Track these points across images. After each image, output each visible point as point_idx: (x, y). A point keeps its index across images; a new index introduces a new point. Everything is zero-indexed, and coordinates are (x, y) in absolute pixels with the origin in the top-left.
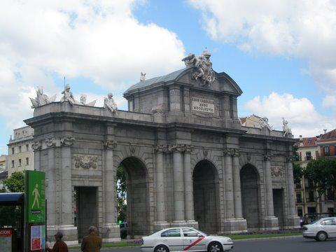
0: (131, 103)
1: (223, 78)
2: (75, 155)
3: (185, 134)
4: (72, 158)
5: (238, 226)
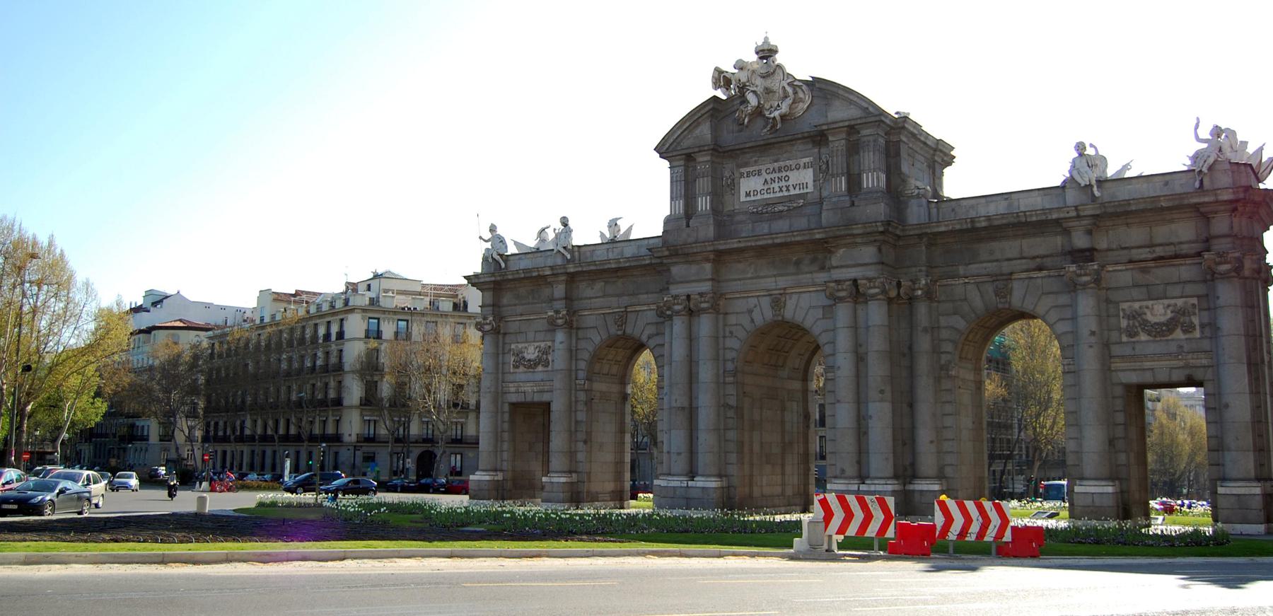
1: (822, 89)
2: (513, 346)
3: (694, 268)
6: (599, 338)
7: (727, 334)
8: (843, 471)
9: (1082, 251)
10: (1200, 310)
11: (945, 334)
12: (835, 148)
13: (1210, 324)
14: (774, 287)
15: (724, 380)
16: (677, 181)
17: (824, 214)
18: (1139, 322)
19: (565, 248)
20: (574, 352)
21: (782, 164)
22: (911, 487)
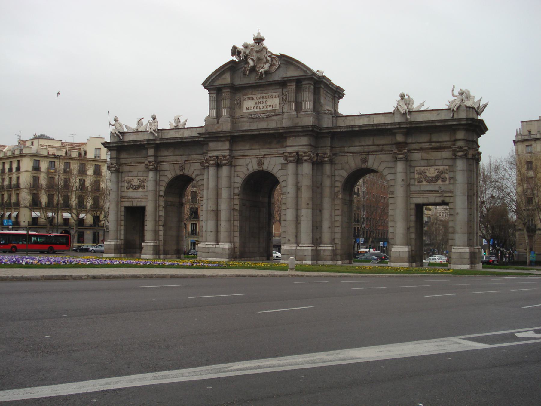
2: (126, 178)
3: (220, 144)
5: (299, 256)
6: (171, 175)
7: (236, 175)
8: (289, 240)
9: (400, 143)
10: (450, 171)
11: (337, 178)
12: (290, 89)
14: (259, 154)
15: (234, 197)
16: (212, 100)
17: (284, 121)
18: (423, 176)
19: (154, 130)
20: (158, 182)
21: (264, 95)
22: (320, 248)
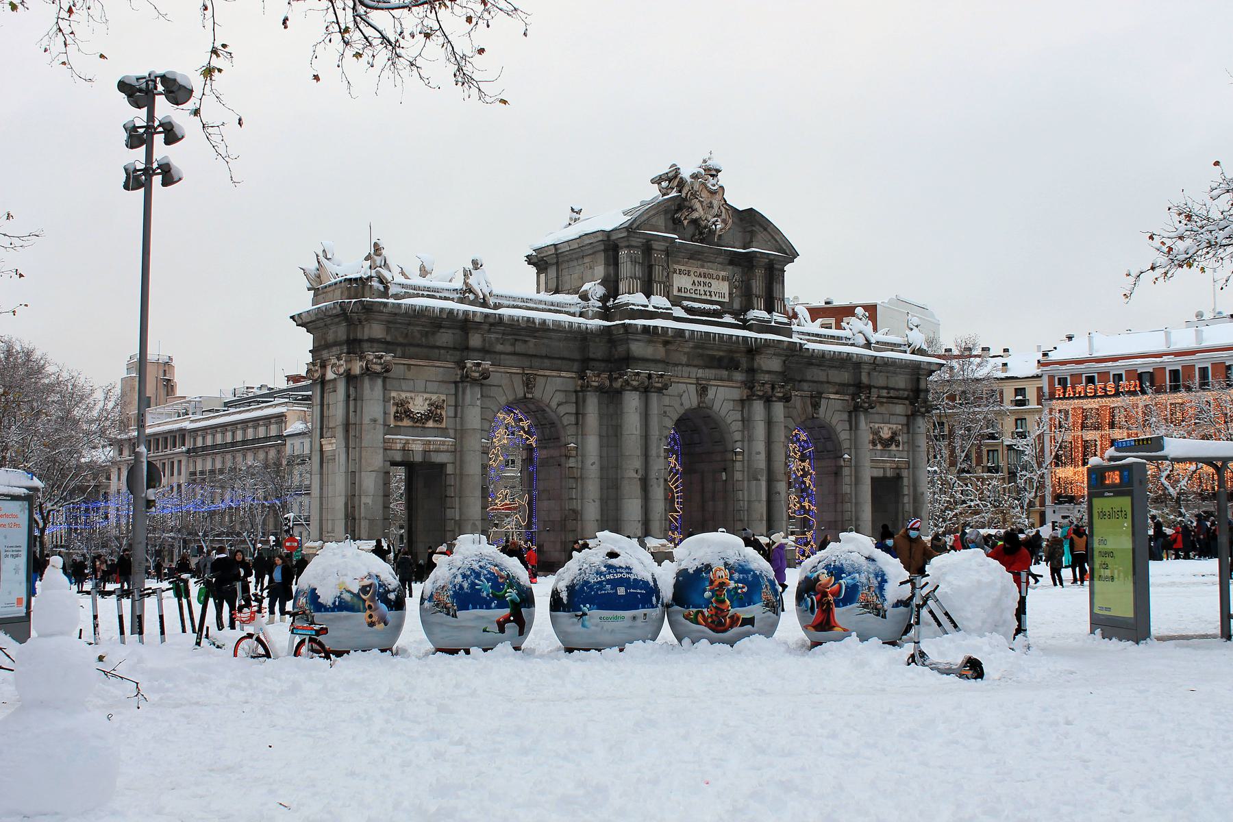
0: (543, 276)
1: (751, 221)
2: (393, 394)
4: (386, 400)
6: (504, 397)
13: (906, 442)
